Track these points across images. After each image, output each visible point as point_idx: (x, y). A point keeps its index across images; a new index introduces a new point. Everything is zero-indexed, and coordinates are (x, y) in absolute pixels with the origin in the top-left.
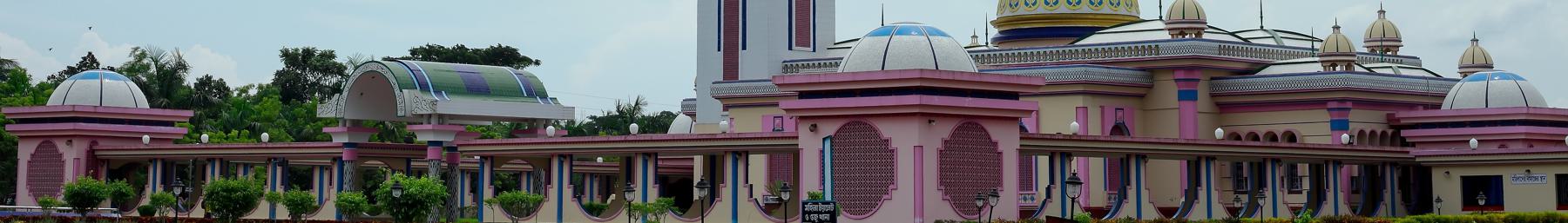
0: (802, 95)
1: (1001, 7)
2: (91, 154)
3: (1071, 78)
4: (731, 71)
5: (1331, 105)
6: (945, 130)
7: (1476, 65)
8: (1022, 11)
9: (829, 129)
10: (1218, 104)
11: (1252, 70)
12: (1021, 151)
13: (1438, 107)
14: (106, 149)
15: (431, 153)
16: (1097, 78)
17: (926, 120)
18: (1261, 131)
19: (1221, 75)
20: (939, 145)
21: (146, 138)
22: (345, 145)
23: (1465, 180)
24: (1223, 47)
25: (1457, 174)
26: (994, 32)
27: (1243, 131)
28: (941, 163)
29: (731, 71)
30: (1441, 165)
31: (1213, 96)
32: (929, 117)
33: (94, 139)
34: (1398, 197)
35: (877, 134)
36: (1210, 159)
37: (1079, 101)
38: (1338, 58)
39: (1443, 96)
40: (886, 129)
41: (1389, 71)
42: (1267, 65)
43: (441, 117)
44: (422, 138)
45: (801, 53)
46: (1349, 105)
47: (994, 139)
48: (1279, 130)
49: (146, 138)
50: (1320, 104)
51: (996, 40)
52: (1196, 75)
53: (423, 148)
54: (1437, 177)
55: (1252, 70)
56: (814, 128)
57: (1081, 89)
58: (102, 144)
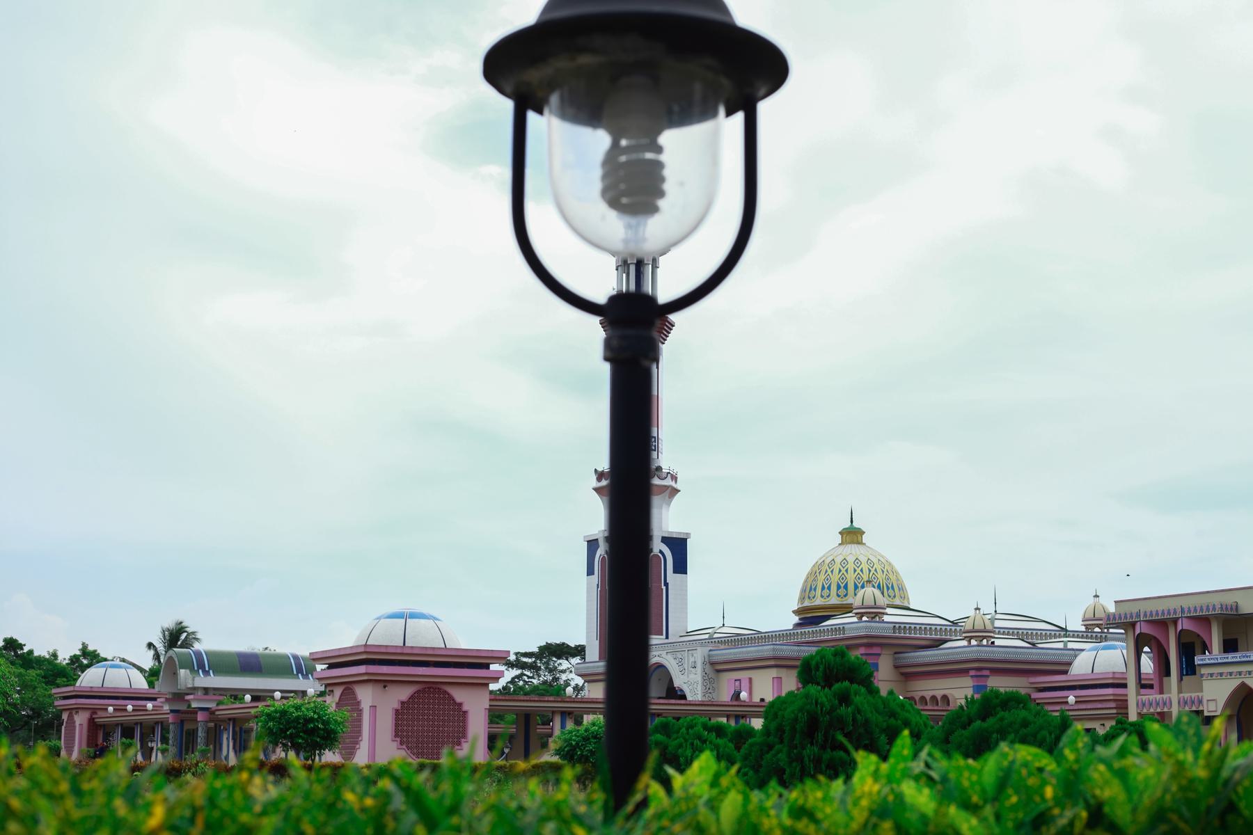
0: (331, 666)
1: (802, 599)
2: (91, 721)
3: (766, 654)
5: (972, 673)
6: (404, 693)
8: (807, 603)
10: (902, 674)
11: (937, 644)
12: (490, 710)
13: (1065, 672)
14: (101, 718)
15: (200, 717)
16: (786, 654)
17: (379, 687)
18: (928, 695)
19: (915, 649)
20: (397, 705)
21: (111, 709)
22: (172, 711)
24: (897, 627)
26: (796, 619)
27: (917, 695)
28: (397, 719)
31: (896, 667)
32: (385, 683)
33: (94, 711)
37: (774, 673)
38: (981, 634)
39: (1070, 664)
41: (1061, 645)
42: (946, 641)
43: (206, 690)
44: (194, 705)
46: (986, 673)
47: (458, 700)
48: (939, 694)
49: (111, 709)
50: (964, 672)
51: (797, 625)
52: (875, 650)
53: (195, 711)
55: (937, 644)
57: (772, 663)
58: (100, 714)
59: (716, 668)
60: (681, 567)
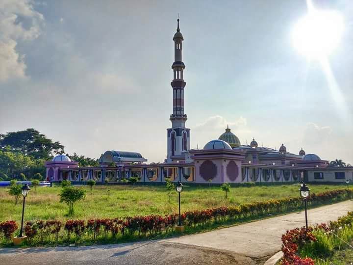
0: (195, 155)
4: (173, 154)
7: (302, 153)
9: (201, 162)
11: (266, 153)
20: (226, 166)
21: (68, 167)
23: (315, 173)
25: (313, 172)
29: (173, 154)
30: (309, 170)
33: (59, 167)
34: (283, 176)
35: (212, 163)
36: (248, 168)
40: (214, 162)
45: (184, 151)
54: (309, 172)
56: (198, 162)
60: (189, 136)
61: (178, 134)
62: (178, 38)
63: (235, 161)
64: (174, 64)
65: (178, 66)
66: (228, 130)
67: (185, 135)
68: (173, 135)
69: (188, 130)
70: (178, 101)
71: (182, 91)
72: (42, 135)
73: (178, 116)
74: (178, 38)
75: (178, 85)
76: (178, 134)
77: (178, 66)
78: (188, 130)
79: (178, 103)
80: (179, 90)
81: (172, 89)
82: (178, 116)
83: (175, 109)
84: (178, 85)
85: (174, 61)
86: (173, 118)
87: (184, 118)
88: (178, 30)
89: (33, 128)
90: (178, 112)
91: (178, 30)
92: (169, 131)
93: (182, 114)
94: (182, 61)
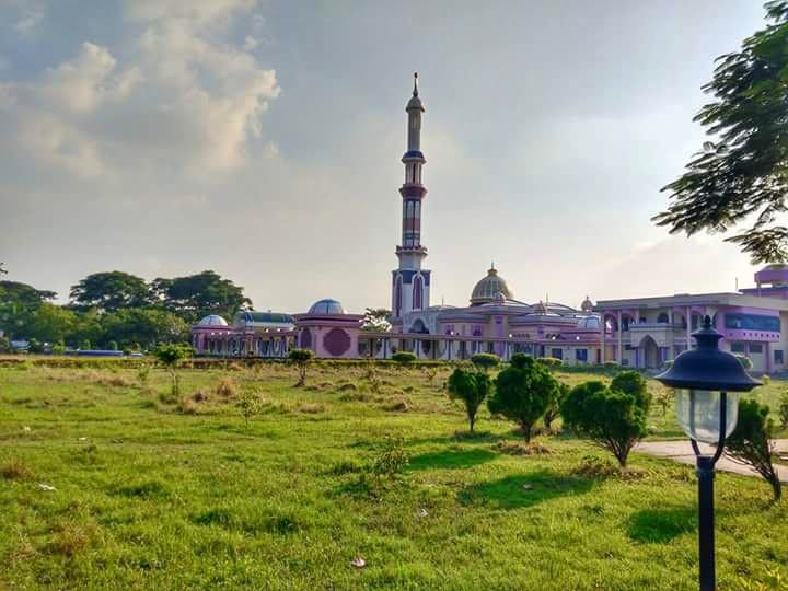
6: (328, 330)
59: (440, 320)
61: (410, 280)
62: (414, 109)
63: (346, 330)
64: (406, 155)
65: (413, 159)
66: (492, 272)
67: (418, 281)
68: (399, 280)
69: (427, 274)
70: (410, 223)
71: (417, 203)
72: (226, 281)
73: (410, 248)
74: (414, 109)
75: (412, 193)
76: (410, 280)
77: (413, 159)
78: (427, 274)
79: (411, 225)
80: (411, 203)
81: (401, 198)
82: (410, 248)
83: (406, 237)
84: (412, 193)
85: (406, 151)
86: (401, 252)
87: (420, 253)
88: (415, 94)
89: (213, 269)
90: (409, 242)
91: (415, 94)
92: (395, 273)
93: (416, 245)
94: (421, 150)
